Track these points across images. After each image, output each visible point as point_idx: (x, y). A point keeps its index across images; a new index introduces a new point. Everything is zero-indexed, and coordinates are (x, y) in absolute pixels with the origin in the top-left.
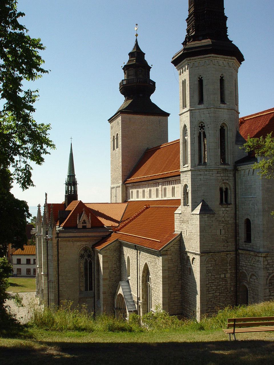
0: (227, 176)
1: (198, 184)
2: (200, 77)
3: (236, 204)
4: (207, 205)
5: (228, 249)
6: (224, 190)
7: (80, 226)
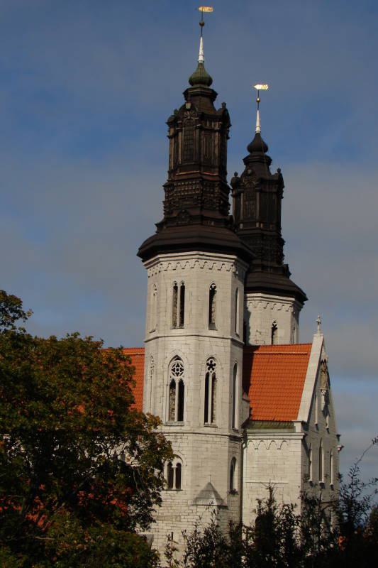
1: (203, 457)
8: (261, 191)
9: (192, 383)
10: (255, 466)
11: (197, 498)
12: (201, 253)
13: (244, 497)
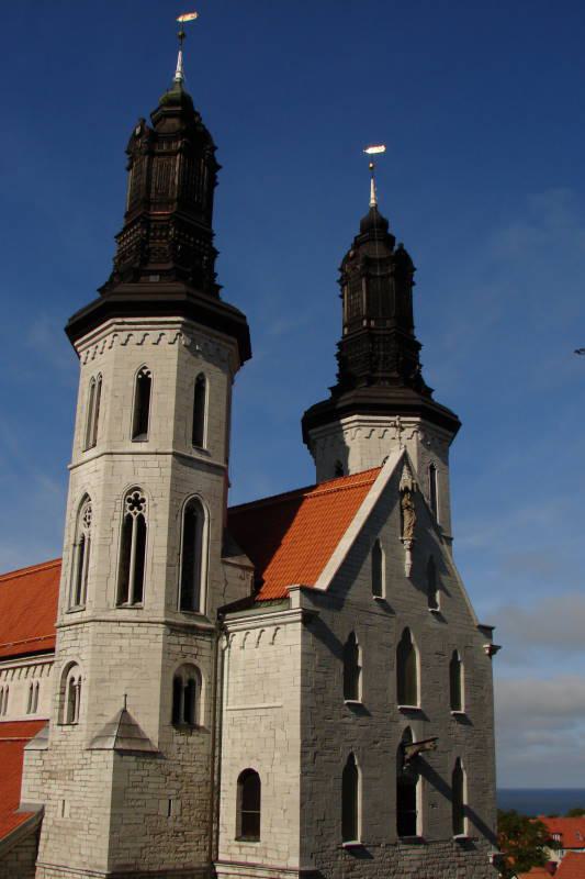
0: (196, 646)
1: (113, 662)
2: (145, 371)
4: (137, 726)
5: (187, 860)
6: (185, 685)
8: (369, 277)
9: (98, 535)
10: (240, 679)
11: (97, 737)
12: (119, 320)
13: (223, 737)
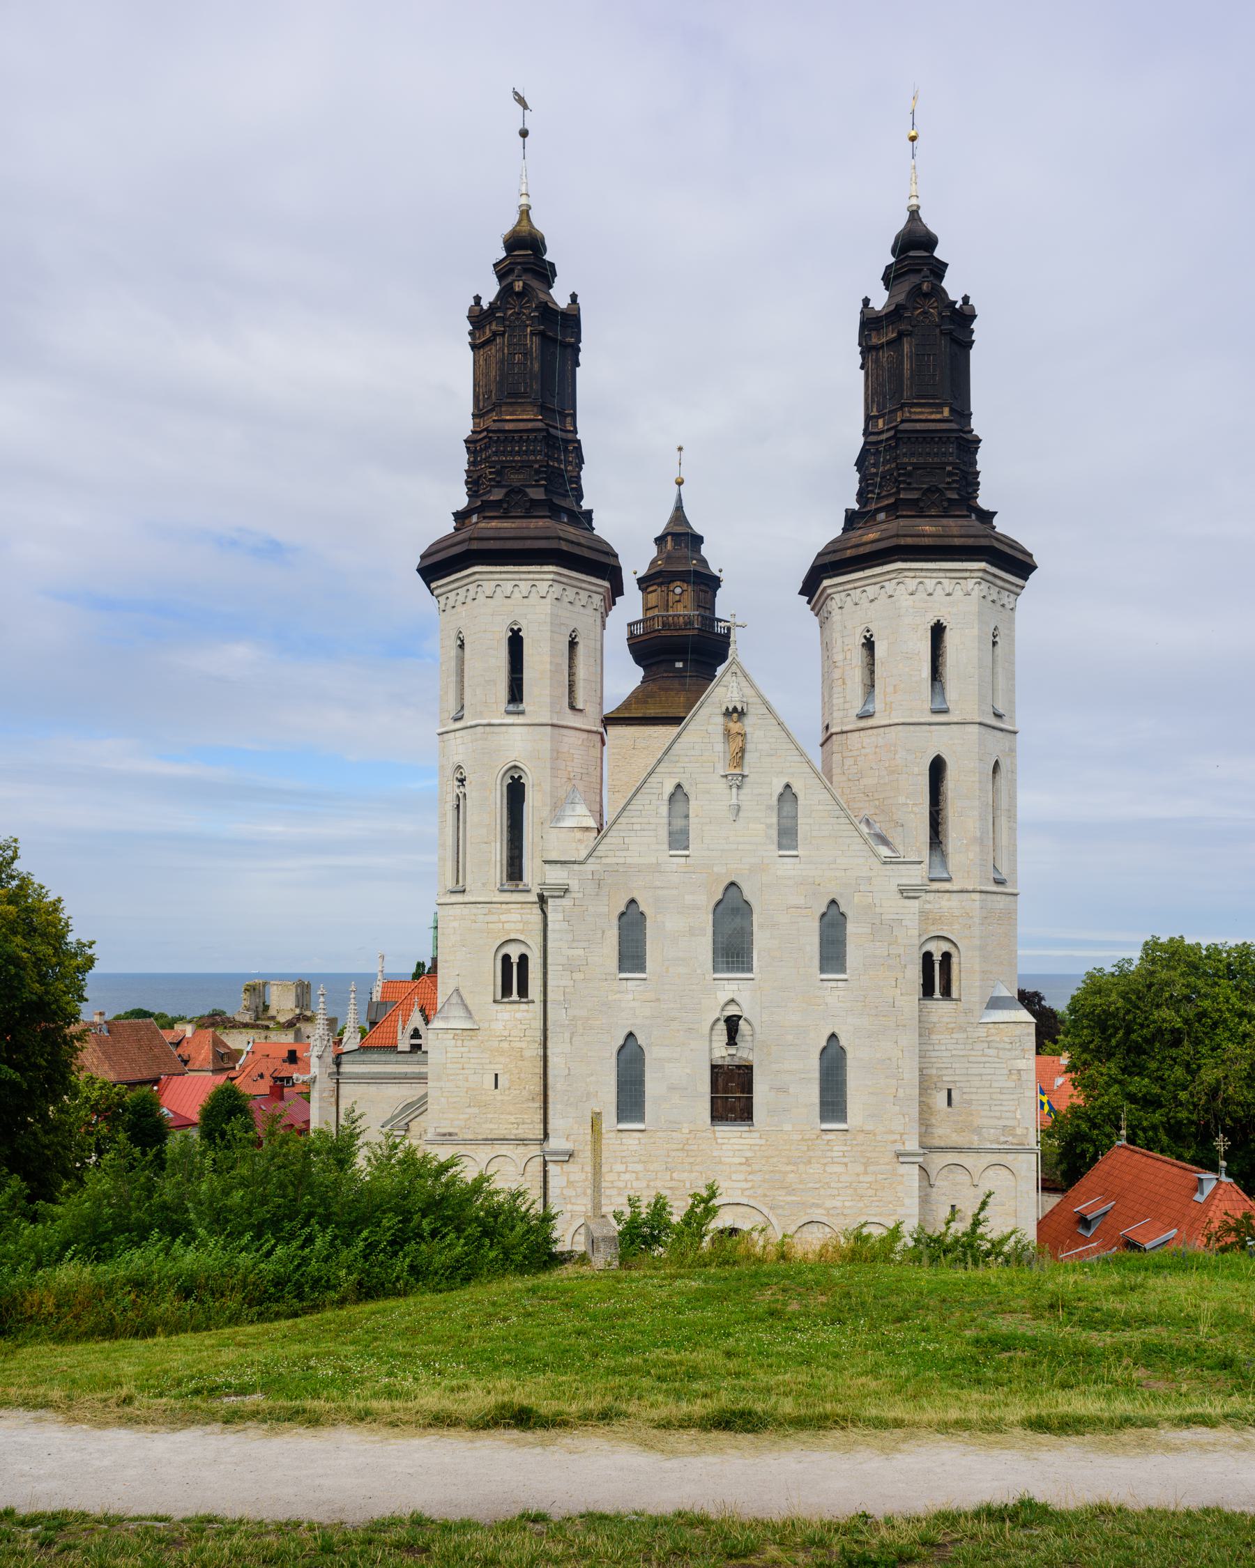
3: (545, 1002)
5: (520, 1131)
6: (515, 959)
7: (404, 1044)
